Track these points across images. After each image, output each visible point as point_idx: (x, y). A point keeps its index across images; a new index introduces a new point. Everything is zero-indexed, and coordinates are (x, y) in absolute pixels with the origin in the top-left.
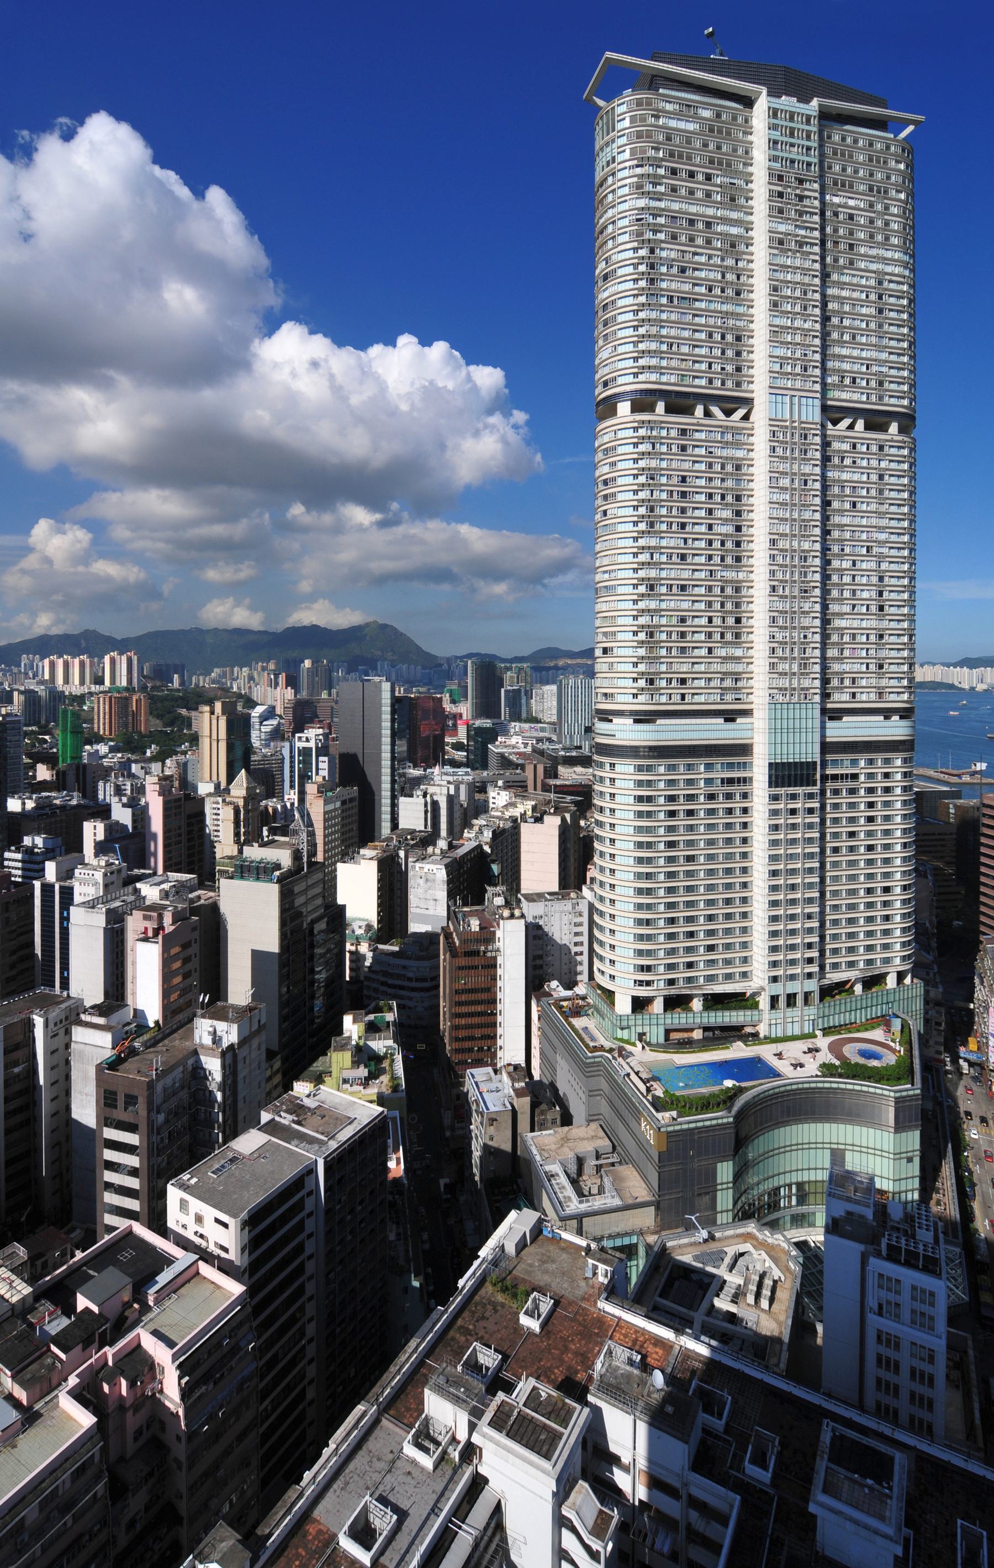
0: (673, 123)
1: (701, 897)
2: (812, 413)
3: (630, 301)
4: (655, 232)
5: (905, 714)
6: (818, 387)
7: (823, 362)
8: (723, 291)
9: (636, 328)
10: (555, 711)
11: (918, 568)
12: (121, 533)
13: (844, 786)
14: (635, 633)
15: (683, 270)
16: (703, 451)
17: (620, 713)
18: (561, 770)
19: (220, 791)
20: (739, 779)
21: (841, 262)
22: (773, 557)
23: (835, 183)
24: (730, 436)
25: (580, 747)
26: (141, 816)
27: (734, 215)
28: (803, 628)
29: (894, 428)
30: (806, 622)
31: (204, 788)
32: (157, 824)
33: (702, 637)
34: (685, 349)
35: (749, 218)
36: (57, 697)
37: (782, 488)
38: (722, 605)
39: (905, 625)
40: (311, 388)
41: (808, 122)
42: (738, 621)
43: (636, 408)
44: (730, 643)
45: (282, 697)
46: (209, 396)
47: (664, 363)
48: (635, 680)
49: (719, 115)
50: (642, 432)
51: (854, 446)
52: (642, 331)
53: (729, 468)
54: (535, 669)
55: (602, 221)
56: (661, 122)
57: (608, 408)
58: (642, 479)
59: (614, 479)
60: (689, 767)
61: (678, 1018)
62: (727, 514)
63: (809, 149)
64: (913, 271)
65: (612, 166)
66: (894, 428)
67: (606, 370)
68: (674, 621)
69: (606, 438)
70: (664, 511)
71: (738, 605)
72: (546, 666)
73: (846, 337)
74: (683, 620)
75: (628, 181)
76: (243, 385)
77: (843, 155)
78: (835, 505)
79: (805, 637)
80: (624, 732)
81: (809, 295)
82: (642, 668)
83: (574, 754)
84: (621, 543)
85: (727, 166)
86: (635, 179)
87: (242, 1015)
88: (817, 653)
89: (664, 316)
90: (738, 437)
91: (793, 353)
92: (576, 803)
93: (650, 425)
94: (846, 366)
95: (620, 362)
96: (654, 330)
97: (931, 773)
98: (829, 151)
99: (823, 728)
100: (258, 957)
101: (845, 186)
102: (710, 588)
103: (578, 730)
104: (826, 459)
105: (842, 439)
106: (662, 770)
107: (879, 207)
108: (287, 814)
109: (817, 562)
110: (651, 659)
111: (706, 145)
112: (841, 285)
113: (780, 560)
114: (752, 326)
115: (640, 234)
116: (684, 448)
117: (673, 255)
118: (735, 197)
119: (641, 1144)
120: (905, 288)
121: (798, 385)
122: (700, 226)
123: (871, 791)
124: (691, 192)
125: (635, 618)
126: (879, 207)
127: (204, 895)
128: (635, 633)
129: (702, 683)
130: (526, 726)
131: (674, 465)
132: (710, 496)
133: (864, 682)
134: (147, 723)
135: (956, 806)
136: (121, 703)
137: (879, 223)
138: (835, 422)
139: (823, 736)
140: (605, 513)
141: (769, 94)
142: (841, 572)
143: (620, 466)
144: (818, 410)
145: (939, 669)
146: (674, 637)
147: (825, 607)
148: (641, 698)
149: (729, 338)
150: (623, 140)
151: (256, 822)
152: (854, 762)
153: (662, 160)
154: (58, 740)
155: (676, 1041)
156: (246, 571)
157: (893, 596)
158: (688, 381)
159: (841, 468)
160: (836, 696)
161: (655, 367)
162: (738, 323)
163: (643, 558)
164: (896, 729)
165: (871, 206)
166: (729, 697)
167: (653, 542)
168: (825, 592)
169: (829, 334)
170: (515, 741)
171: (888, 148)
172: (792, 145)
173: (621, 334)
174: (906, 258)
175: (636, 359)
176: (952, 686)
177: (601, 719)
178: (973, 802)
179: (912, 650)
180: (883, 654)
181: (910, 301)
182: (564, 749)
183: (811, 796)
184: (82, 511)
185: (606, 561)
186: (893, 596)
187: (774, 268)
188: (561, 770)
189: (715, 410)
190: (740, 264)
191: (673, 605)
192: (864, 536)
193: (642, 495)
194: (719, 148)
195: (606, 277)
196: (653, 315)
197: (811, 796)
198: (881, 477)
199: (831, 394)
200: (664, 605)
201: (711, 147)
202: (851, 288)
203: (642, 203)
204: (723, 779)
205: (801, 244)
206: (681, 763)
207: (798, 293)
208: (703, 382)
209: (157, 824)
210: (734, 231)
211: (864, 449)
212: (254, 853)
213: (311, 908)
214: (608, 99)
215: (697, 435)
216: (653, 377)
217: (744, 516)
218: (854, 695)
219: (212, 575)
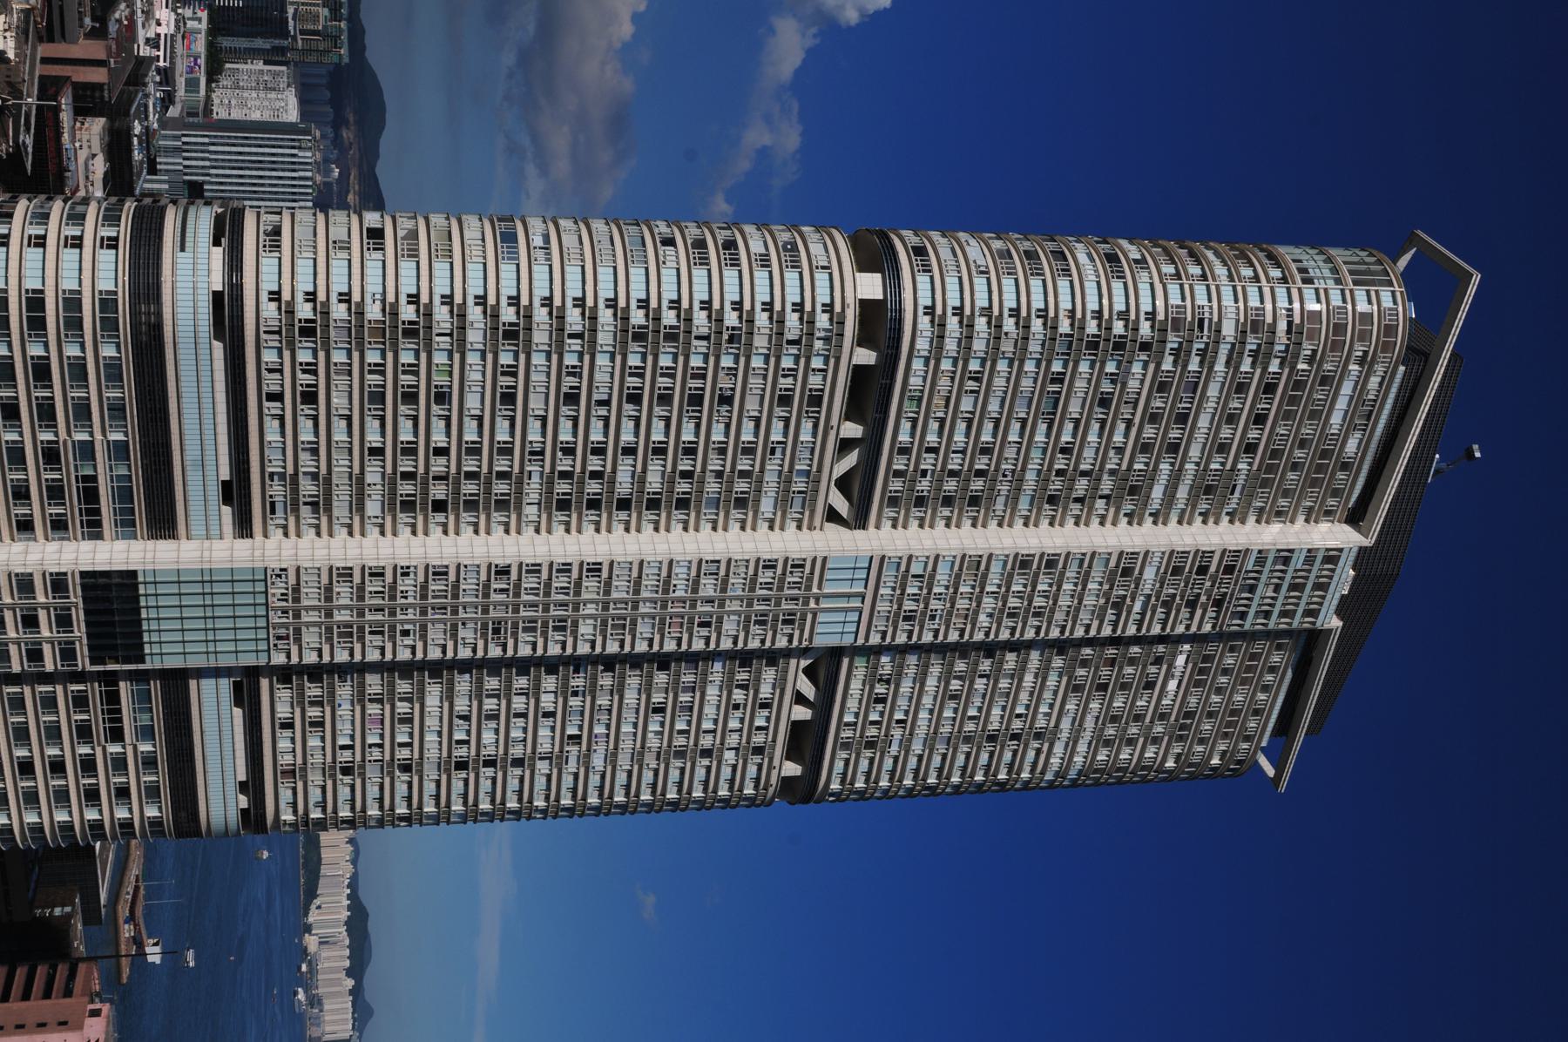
0: (1347, 388)
2: (830, 632)
3: (1065, 304)
4: (1176, 353)
5: (253, 818)
6: (875, 639)
7: (918, 649)
8: (1060, 473)
9: (1015, 313)
10: (236, 115)
11: (537, 823)
13: (96, 715)
14: (414, 299)
15: (1104, 402)
16: (776, 436)
17: (234, 262)
18: (97, 125)
20: (98, 512)
21: (1081, 672)
22: (565, 569)
23: (1207, 659)
24: (801, 487)
25: (153, 170)
27: (1182, 493)
28: (424, 628)
29: (792, 769)
30: (436, 634)
33: (406, 436)
34: (966, 404)
35: (1174, 518)
37: (696, 582)
38: (471, 476)
39: (429, 808)
41: (1283, 614)
42: (440, 506)
43: (868, 308)
44: (393, 491)
47: (946, 365)
48: (311, 297)
49: (1345, 466)
50: (822, 320)
51: (764, 706)
52: (1009, 324)
53: (741, 486)
54: (338, 76)
55: (1210, 255)
56: (1354, 367)
57: (874, 254)
58: (731, 319)
59: (735, 263)
60: (117, 410)
62: (654, 482)
63: (1267, 615)
64: (1074, 783)
65: (1298, 278)
66: (792, 769)
67: (945, 253)
68: (439, 379)
69: (816, 249)
70: (666, 361)
71: (471, 505)
72: (345, 100)
73: (955, 685)
74: (442, 397)
75: (1269, 306)
77: (1249, 669)
78: (661, 678)
79: (406, 633)
80: (192, 271)
81: (1033, 621)
82: (339, 311)
83: (137, 156)
84: (605, 274)
85: (1259, 481)
86: (1269, 319)
88: (373, 656)
89: (1029, 366)
90: (798, 501)
91: (939, 597)
92: (17, 154)
93: (834, 338)
94: (906, 686)
95: (959, 281)
96: (1007, 347)
97: (134, 870)
98: (1257, 647)
99: (217, 673)
101: (1199, 676)
102: (506, 451)
103: (195, 165)
104: (745, 658)
105: (779, 684)
106: (108, 351)
107: (1158, 729)
109: (554, 650)
110: (357, 330)
111: (1303, 444)
112: (1042, 674)
113: (559, 582)
114: (993, 524)
115: (1177, 324)
116: (785, 400)
117: (1133, 384)
118: (1212, 495)
120: (1025, 775)
121: (883, 606)
122: (1174, 434)
123: (88, 765)
124: (1232, 419)
125: (448, 300)
126: (1158, 729)
128: (414, 299)
129: (306, 436)
130: (200, 46)
131: (755, 382)
132: (690, 451)
133: (314, 742)
135: (69, 916)
137: (1133, 730)
138: (808, 672)
139: (200, 673)
140: (669, 242)
141: (1362, 550)
142: (535, 692)
143: (761, 276)
144: (833, 641)
145: (347, 870)
146: (406, 379)
147: (465, 666)
148: (270, 310)
149: (977, 484)
150: (1336, 300)
152: (147, 733)
153: (1293, 368)
157: (486, 785)
158: (909, 407)
159: (728, 685)
160: (283, 694)
161: (940, 347)
162: (1001, 501)
163: (574, 318)
164: (220, 802)
165: (1163, 717)
166: (277, 490)
167: (605, 338)
168: (494, 667)
169: (963, 656)
171: (1248, 739)
172: (1277, 588)
173: (1008, 283)
174: (1072, 774)
175: (959, 311)
176: (312, 894)
177: (219, 222)
178: (79, 947)
179: (381, 823)
180: (373, 773)
181: (1002, 785)
182: (148, 134)
183: (68, 653)
185: (569, 240)
186: (486, 785)
187: (1086, 562)
188: (97, 125)
189: (851, 459)
190: (1100, 504)
191: (474, 376)
192: (599, 730)
193: (700, 318)
194: (1295, 467)
195: (1112, 258)
196: (1034, 347)
197: (68, 653)
198: (707, 753)
199: (860, 662)
200: (473, 358)
201: (1298, 453)
202: (1037, 689)
203: (1228, 330)
204: (94, 478)
205: (1118, 606)
206: (127, 391)
207: (1038, 602)
208: (904, 437)
210: (1157, 492)
211: (760, 722)
214: (1407, 276)
215: (807, 426)
216: (922, 345)
217: (649, 515)
218: (288, 725)
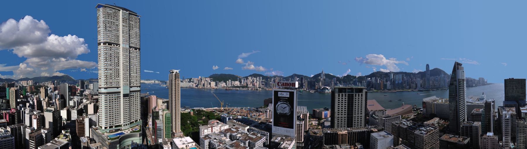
1: (114, 113)
12: (30, 64)
19: (44, 100)
26: (34, 103)
31: (42, 99)
32: (36, 104)
36: (23, 86)
40: (56, 42)
45: (52, 86)
46: (41, 45)
61: (111, 129)
76: (46, 43)
80: (103, 90)
87: (47, 129)
100: (49, 122)
108: (53, 103)
119: (106, 144)
127: (42, 114)
134: (34, 90)
136: (31, 87)
151: (49, 104)
154: (23, 92)
155: (110, 132)
156: (47, 68)
170: (87, 92)
184: (25, 62)
209: (36, 104)
212: (49, 108)
213: (57, 116)
219: (42, 69)
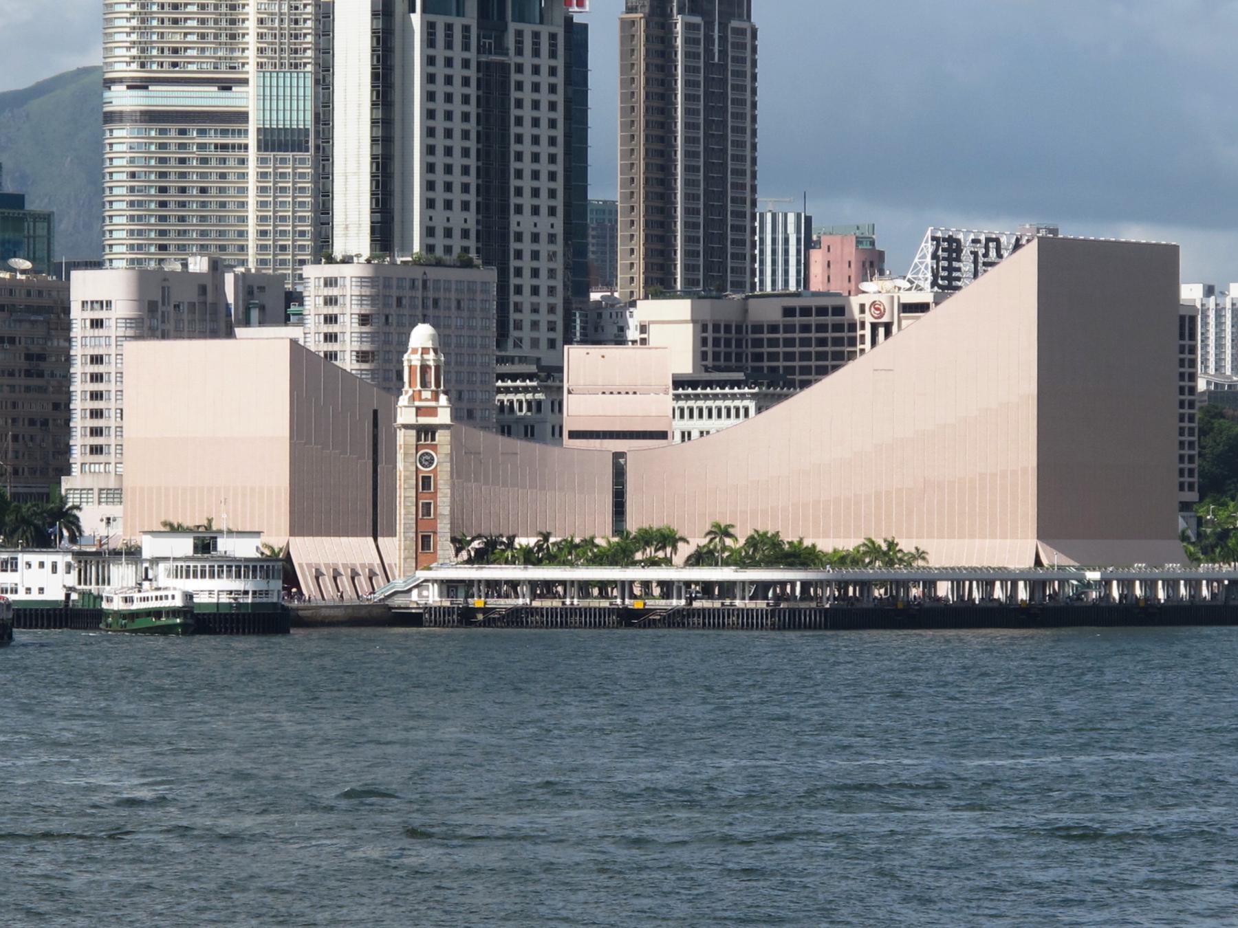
20: (233, 147)
148: (134, 66)
204: (216, 146)
206: (173, 127)
